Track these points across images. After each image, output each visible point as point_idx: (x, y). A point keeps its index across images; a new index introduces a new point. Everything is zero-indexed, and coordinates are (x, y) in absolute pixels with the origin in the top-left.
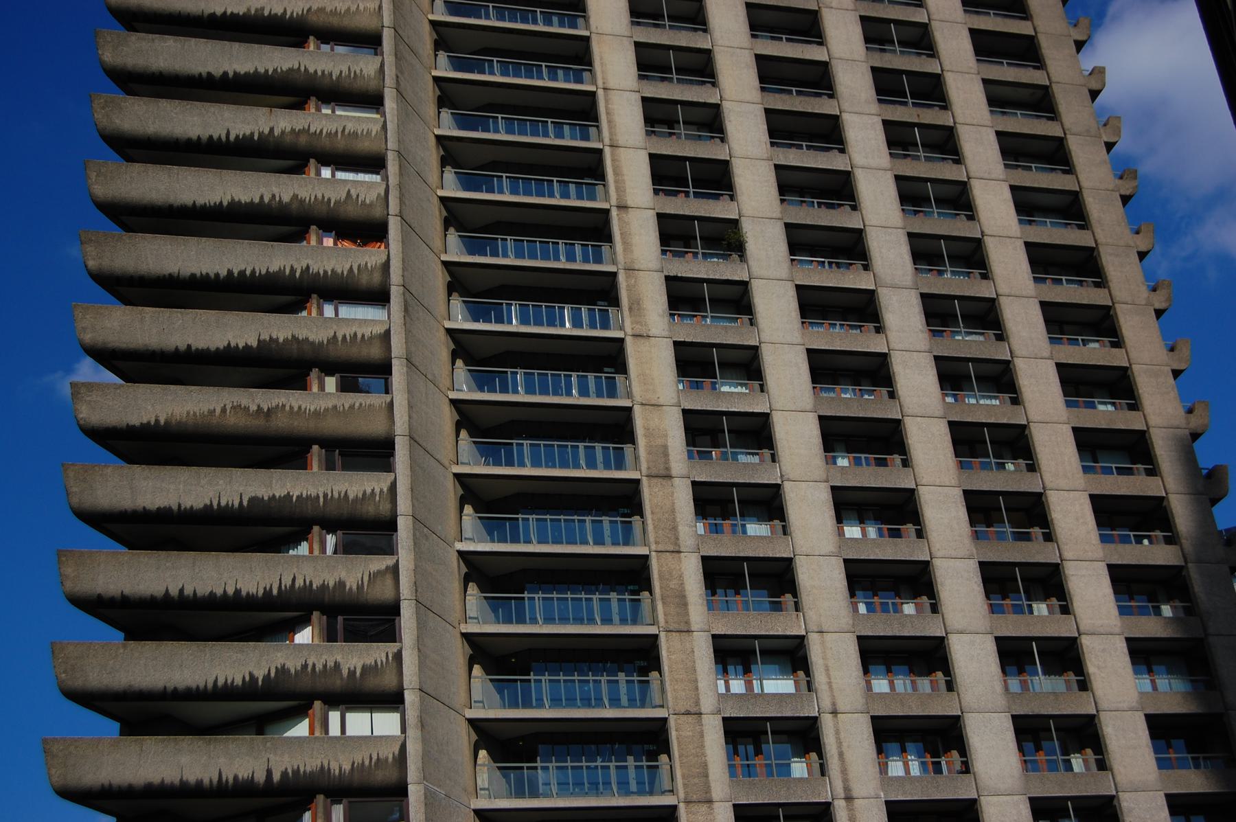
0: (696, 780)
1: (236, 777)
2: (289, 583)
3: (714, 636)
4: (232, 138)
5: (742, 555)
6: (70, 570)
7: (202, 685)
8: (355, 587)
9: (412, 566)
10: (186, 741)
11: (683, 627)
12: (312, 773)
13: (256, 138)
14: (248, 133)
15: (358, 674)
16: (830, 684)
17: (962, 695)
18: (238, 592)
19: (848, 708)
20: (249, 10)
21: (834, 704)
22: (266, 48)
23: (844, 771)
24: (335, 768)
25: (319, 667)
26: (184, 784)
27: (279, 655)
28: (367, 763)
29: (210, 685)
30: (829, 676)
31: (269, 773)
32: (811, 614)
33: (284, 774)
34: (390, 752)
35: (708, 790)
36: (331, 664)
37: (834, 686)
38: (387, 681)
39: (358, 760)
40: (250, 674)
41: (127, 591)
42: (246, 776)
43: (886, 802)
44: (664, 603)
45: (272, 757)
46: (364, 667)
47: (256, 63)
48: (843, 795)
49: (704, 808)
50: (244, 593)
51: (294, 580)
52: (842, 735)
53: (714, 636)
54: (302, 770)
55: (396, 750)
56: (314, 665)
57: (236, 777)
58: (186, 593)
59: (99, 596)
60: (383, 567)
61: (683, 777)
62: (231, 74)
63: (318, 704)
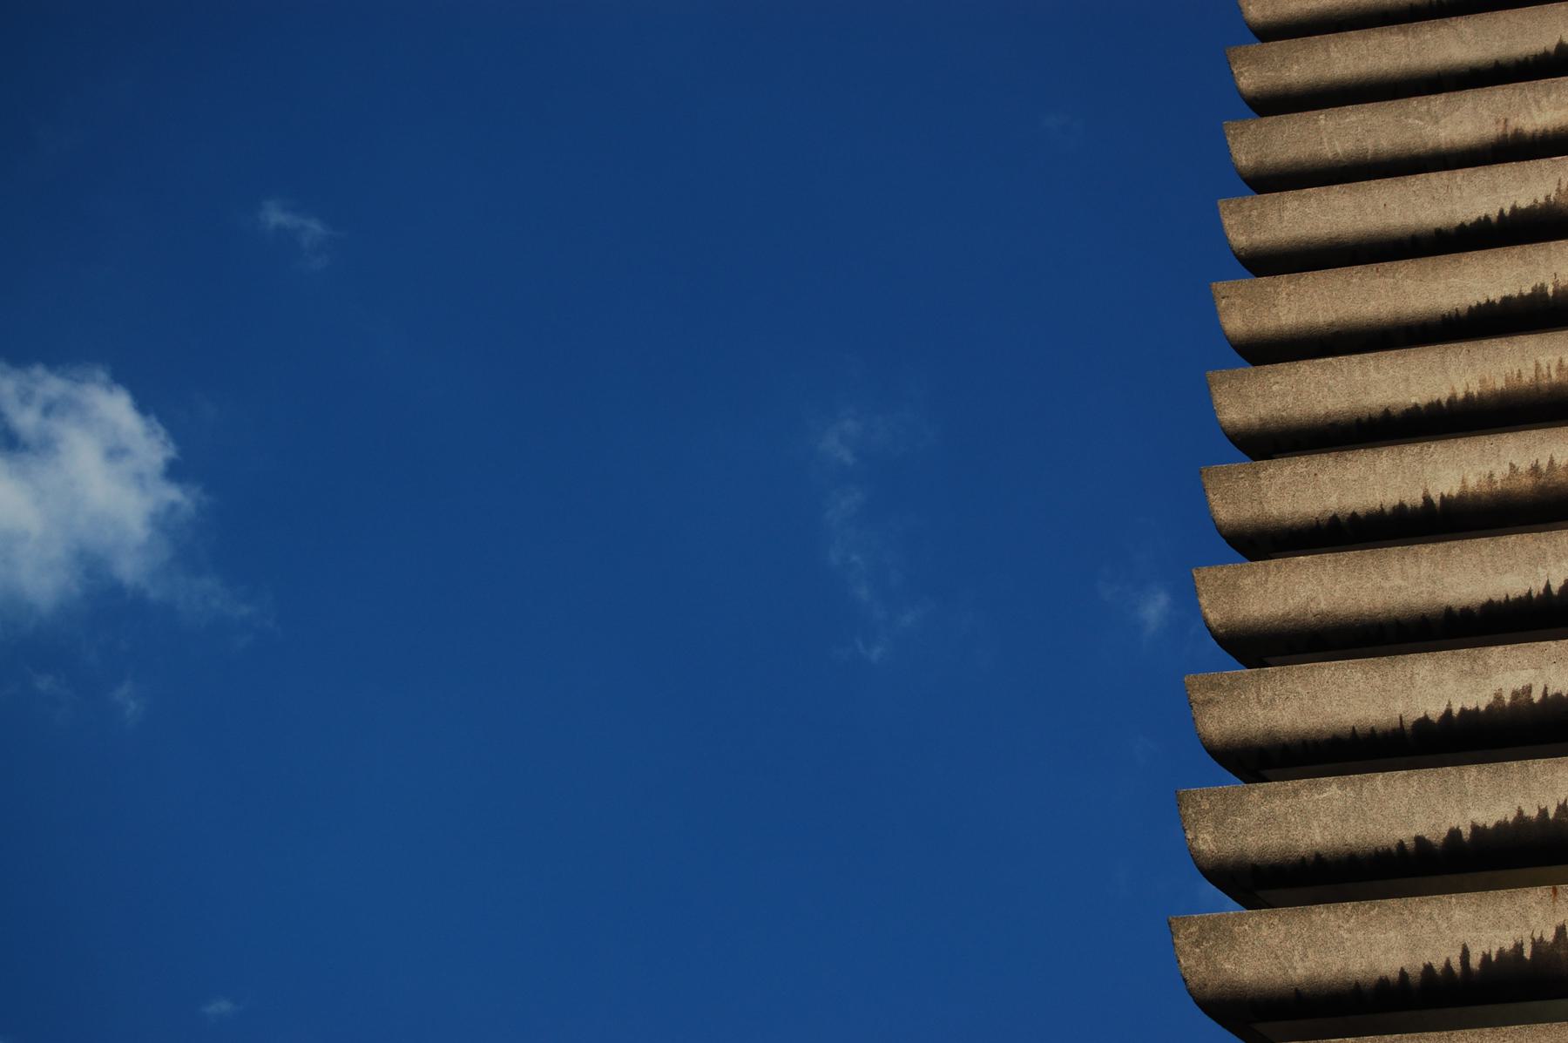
4: (1475, 961)
13: (1527, 954)
14: (1508, 945)
20: (1498, 697)
22: (1537, 766)
47: (1520, 801)
62: (1466, 832)
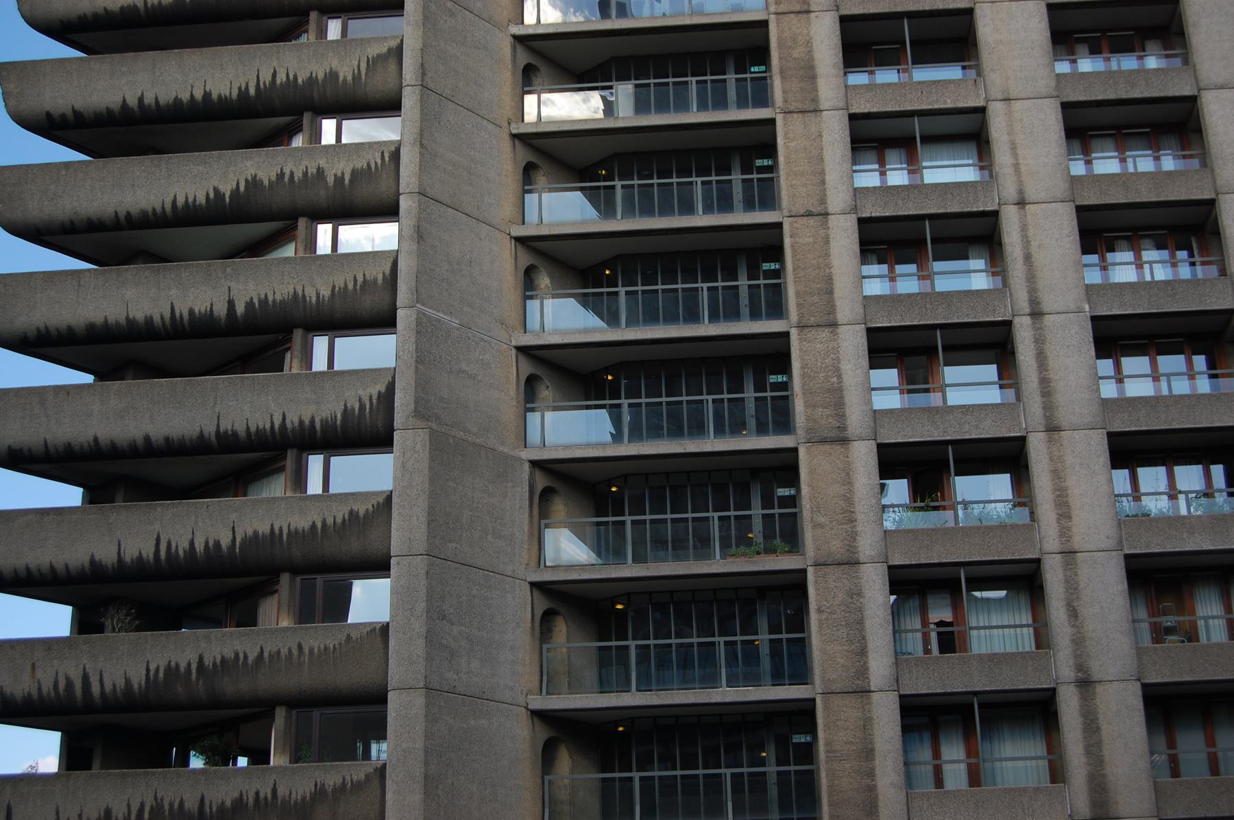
0: (816, 299)
1: (191, 312)
2: (269, 79)
3: (853, 117)
5: (899, 9)
6: (12, 86)
7: (159, 209)
8: (350, 78)
9: (419, 45)
10: (129, 271)
11: (808, 106)
12: (283, 302)
15: (347, 181)
16: (1016, 166)
17: (1218, 171)
18: (207, 95)
19: (1042, 196)
21: (1021, 192)
23: (1031, 278)
24: (311, 294)
25: (298, 175)
26: (131, 322)
27: (249, 163)
28: (351, 286)
29: (168, 207)
30: (1015, 155)
31: (231, 304)
32: (994, 78)
33: (250, 305)
34: (378, 272)
35: (831, 308)
36: (312, 170)
37: (1023, 168)
38: (383, 187)
39: (340, 283)
40: (216, 190)
41: (78, 106)
42: (203, 310)
43: (1095, 319)
44: (783, 78)
45: (233, 285)
46: (354, 173)
48: (1027, 310)
49: (824, 334)
50: (215, 96)
51: (274, 75)
52: (1031, 232)
53: (853, 117)
54: (270, 299)
55: (387, 269)
56: (292, 173)
57: (191, 312)
58: (146, 101)
59: (48, 114)
60: (385, 50)
61: (798, 294)
63: (302, 223)
